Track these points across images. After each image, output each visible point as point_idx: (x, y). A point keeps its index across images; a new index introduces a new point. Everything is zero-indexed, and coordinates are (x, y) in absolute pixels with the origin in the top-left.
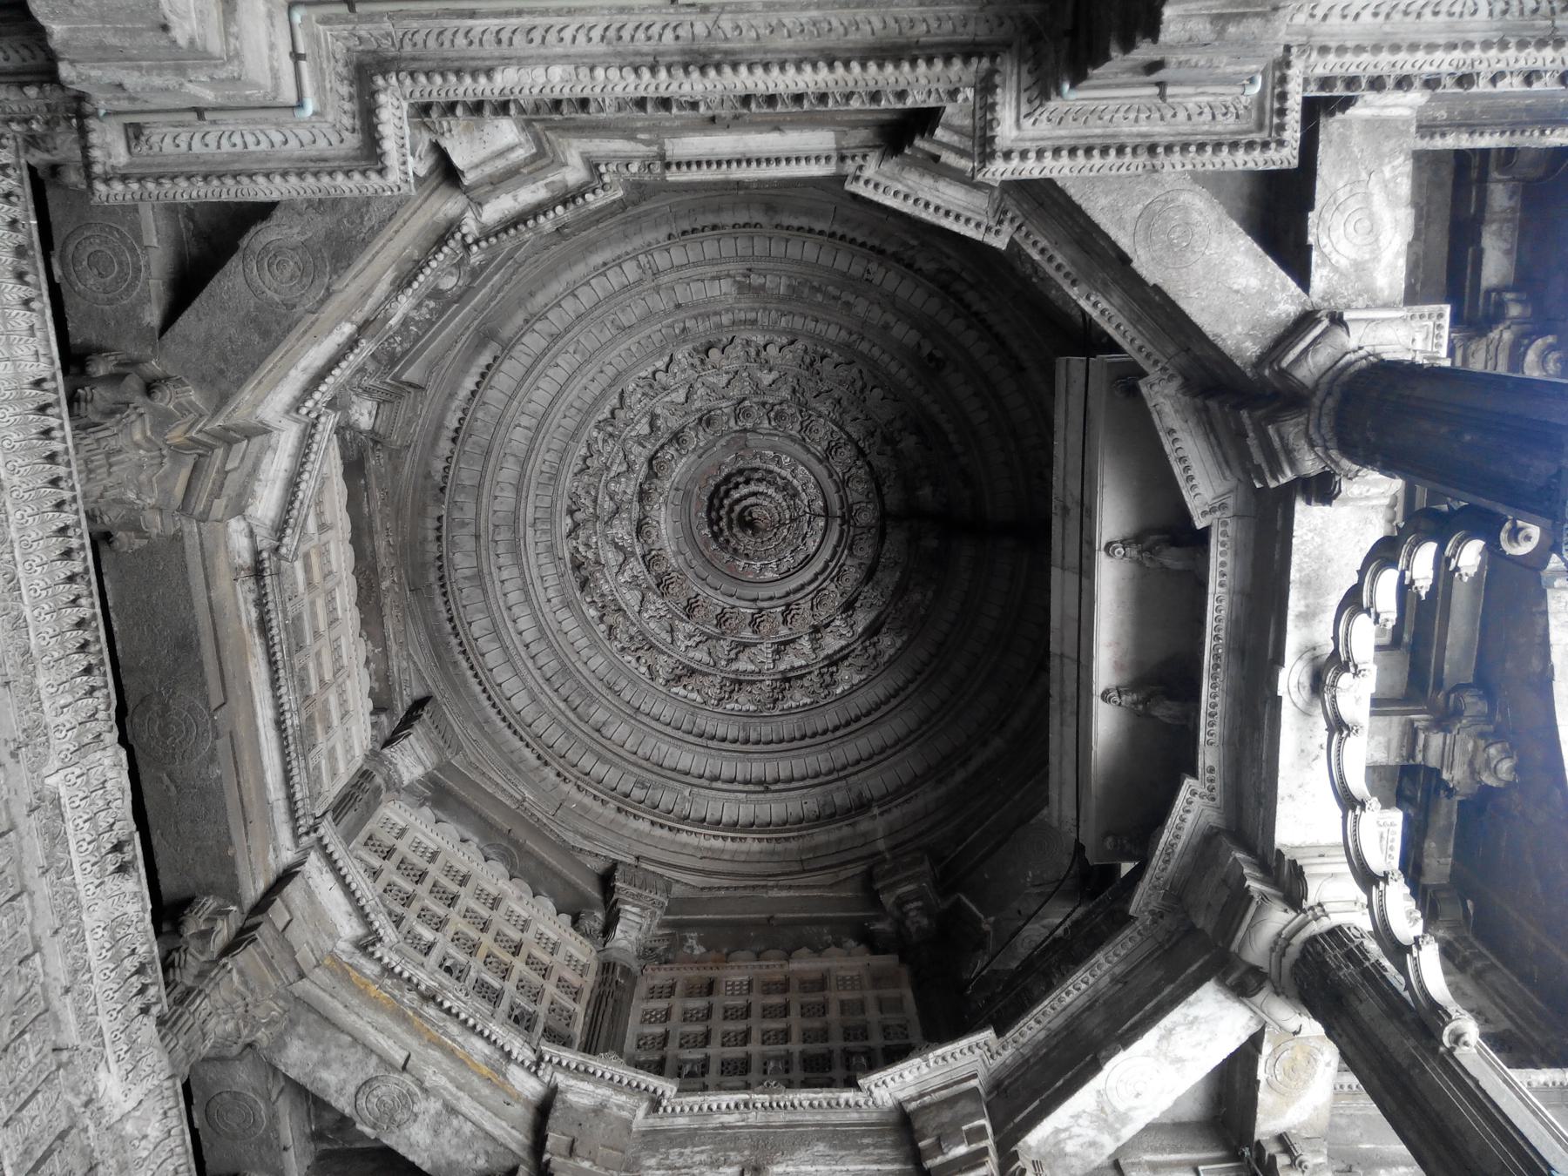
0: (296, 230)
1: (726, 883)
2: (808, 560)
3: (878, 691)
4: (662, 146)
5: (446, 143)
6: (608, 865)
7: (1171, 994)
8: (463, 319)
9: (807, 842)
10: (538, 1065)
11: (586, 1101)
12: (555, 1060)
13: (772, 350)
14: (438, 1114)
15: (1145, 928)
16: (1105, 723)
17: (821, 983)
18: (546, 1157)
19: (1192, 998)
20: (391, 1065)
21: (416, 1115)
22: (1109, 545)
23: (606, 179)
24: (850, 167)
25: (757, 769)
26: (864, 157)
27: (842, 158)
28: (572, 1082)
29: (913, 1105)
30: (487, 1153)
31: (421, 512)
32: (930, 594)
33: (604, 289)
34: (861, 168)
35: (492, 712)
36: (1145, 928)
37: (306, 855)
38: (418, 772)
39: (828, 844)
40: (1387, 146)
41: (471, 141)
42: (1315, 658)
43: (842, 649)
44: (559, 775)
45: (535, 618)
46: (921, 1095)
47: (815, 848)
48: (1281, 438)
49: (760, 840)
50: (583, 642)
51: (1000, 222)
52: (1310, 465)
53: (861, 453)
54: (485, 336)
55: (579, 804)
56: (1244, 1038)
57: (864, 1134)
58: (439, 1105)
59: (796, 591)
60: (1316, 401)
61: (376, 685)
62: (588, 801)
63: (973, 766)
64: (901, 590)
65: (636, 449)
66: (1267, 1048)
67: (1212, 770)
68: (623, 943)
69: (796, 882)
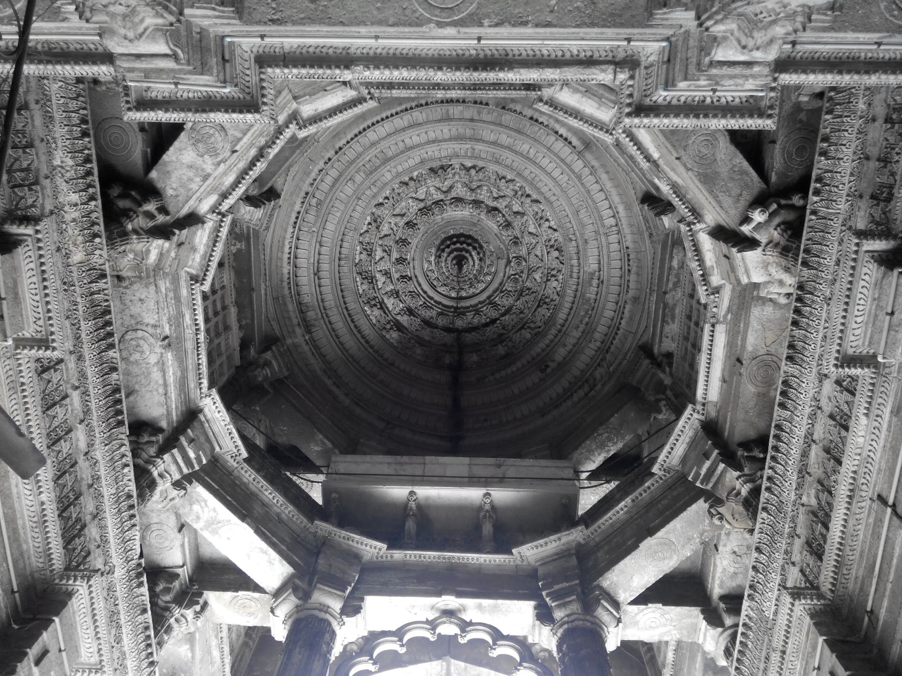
0: (723, 157)
1: (267, 258)
2: (434, 287)
3: (367, 330)
4: (722, 323)
5: (759, 250)
6: (279, 191)
7: (283, 550)
9: (288, 300)
10: (219, 213)
11: (197, 240)
12: (223, 224)
13: (555, 284)
14: (203, 170)
15: (308, 529)
16: (398, 492)
17: (227, 328)
18: (177, 232)
19: (284, 562)
20: (236, 145)
21: (202, 156)
22: (489, 494)
23: (712, 297)
24: (699, 407)
25: (325, 266)
26: (703, 414)
27: (704, 405)
28: (207, 231)
29: (203, 419)
30: (177, 196)
32: (419, 358)
33: (602, 206)
34: (698, 412)
35: (369, 123)
36: (308, 529)
37: (356, 89)
39: (288, 312)
40: (685, 632)
41: (757, 262)
42: (460, 611)
43: (387, 308)
45: (418, 146)
46: (207, 421)
47: (285, 304)
48: (570, 602)
49: (289, 273)
50: (400, 169)
51: (665, 470)
52: (558, 614)
53: (493, 321)
55: (312, 170)
56: (261, 585)
57: (185, 393)
58: (209, 171)
59: (418, 281)
60: (588, 618)
62: (313, 175)
63: (334, 389)
64: (421, 342)
65: (504, 204)
66: (257, 595)
67: (392, 557)
68: (243, 211)
69: (268, 297)
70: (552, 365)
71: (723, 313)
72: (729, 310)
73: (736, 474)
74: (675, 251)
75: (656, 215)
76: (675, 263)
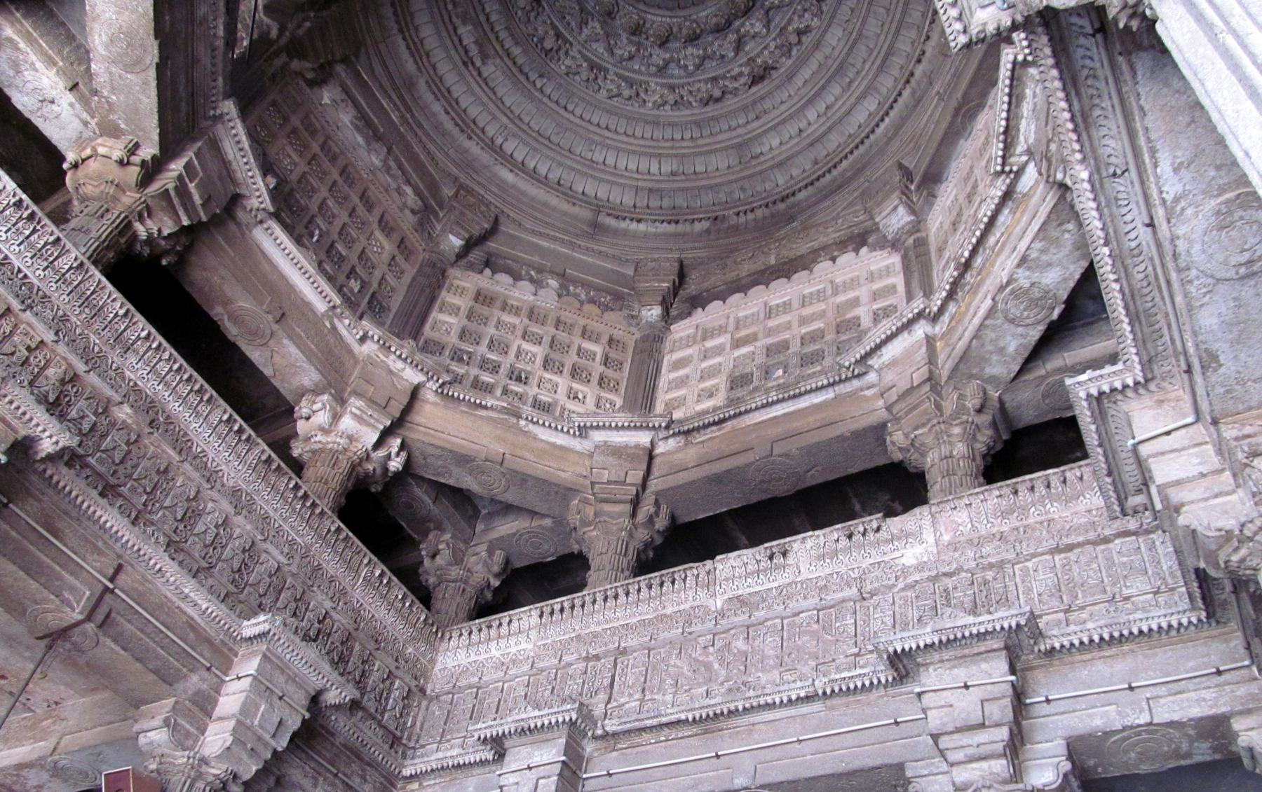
5: (370, 448)
8: (584, 254)
14: (1029, 269)
31: (736, 228)
33: (533, 157)
38: (901, 210)
44: (919, 61)
50: (819, 56)
54: (596, 228)
58: (1020, 271)
61: (850, 248)
71: (336, 321)
72: (334, 328)
73: (166, 232)
74: (420, 203)
75: (471, 237)
76: (409, 190)
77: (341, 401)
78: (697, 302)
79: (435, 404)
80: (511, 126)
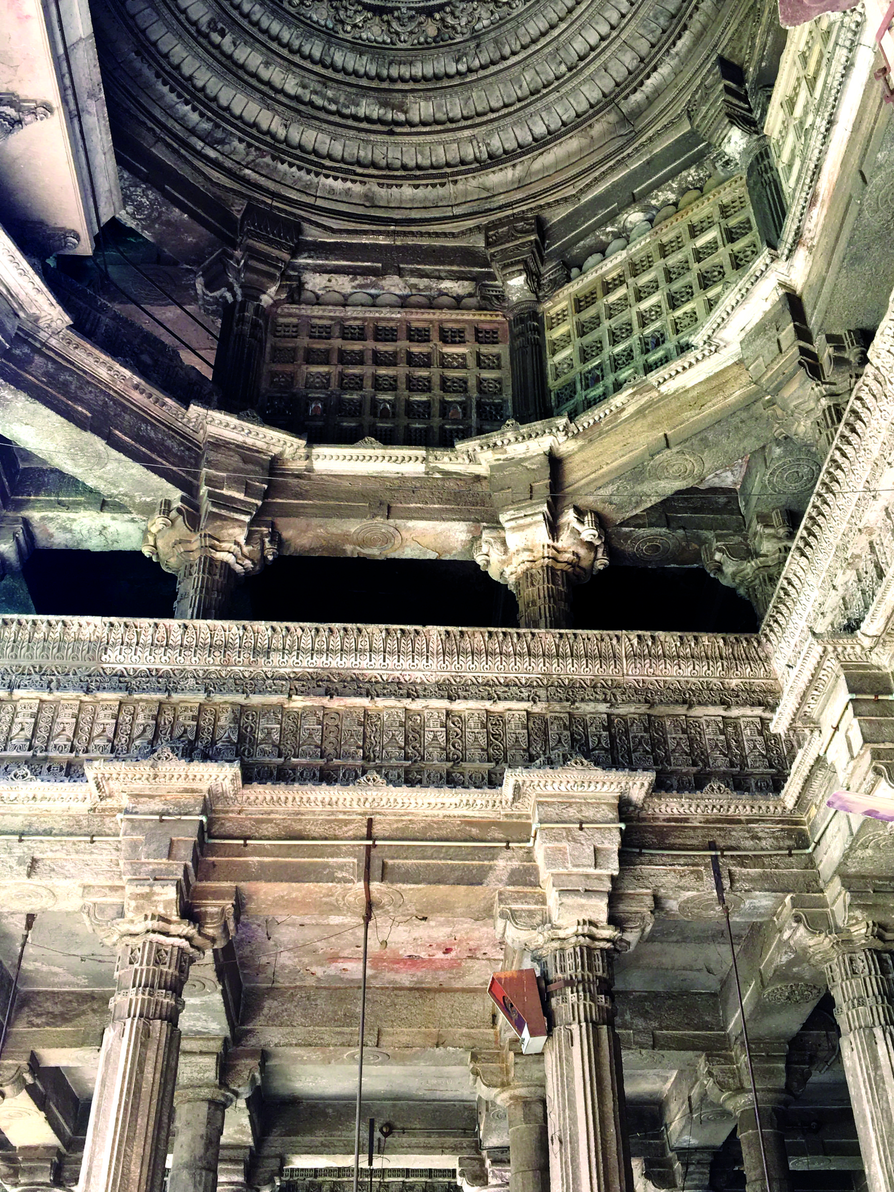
70: (227, 43)
74: (466, 283)
77: (496, 525)
78: (767, 81)
79: (582, 448)
80: (476, 131)
